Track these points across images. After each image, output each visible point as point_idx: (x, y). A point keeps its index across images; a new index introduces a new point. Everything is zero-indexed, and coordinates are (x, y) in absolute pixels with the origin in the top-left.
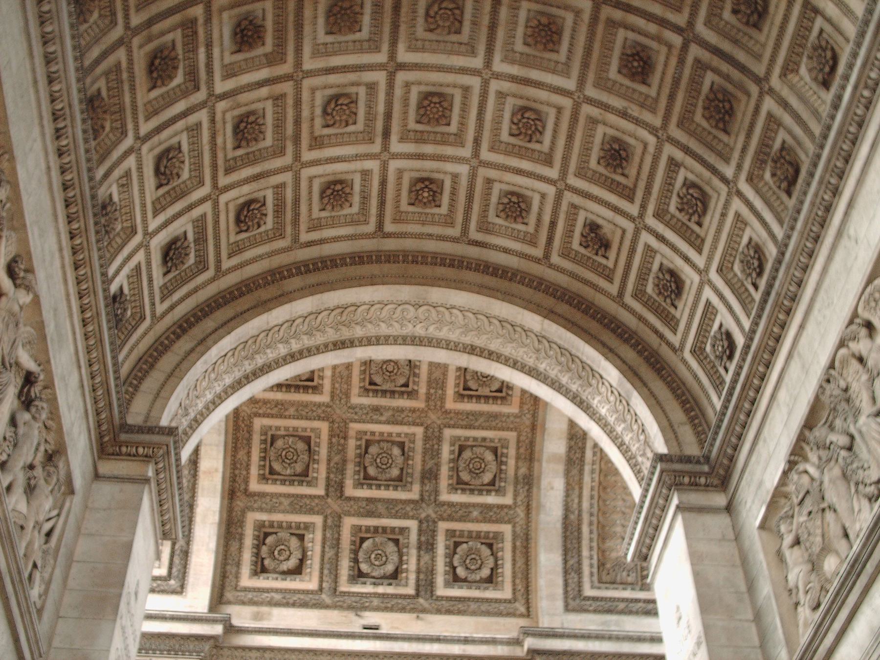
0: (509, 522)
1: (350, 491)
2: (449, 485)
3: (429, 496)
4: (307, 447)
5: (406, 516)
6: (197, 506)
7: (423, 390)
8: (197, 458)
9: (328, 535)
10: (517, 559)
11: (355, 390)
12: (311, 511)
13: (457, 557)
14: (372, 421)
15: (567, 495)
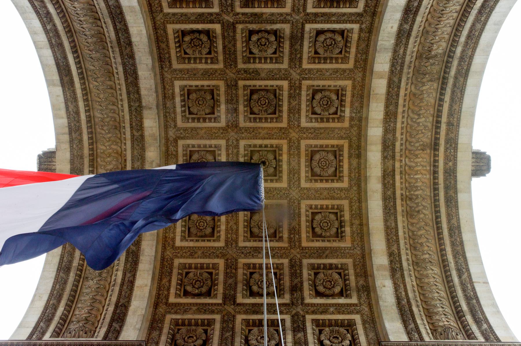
0: (357, 313)
1: (240, 299)
2: (310, 294)
6: (130, 306)
8: (134, 280)
11: (241, 238)
12: (212, 312)
14: (253, 257)
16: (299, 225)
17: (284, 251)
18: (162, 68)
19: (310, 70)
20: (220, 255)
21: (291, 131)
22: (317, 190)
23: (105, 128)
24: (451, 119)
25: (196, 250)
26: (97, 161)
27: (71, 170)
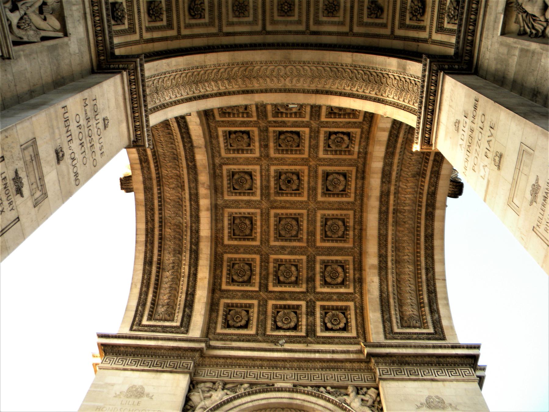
0: (352, 300)
1: (271, 288)
2: (321, 284)
3: (311, 289)
4: (249, 268)
5: (300, 299)
6: (196, 294)
7: (305, 237)
8: (197, 273)
9: (261, 309)
10: (358, 318)
11: (272, 239)
12: (252, 298)
13: (327, 318)
14: (281, 254)
15: (381, 285)
16: (315, 228)
17: (303, 249)
18: (207, 120)
19: (327, 122)
20: (257, 252)
21: (311, 159)
22: (329, 203)
23: (166, 159)
24: (437, 158)
25: (239, 248)
26: (162, 181)
27: (144, 188)
